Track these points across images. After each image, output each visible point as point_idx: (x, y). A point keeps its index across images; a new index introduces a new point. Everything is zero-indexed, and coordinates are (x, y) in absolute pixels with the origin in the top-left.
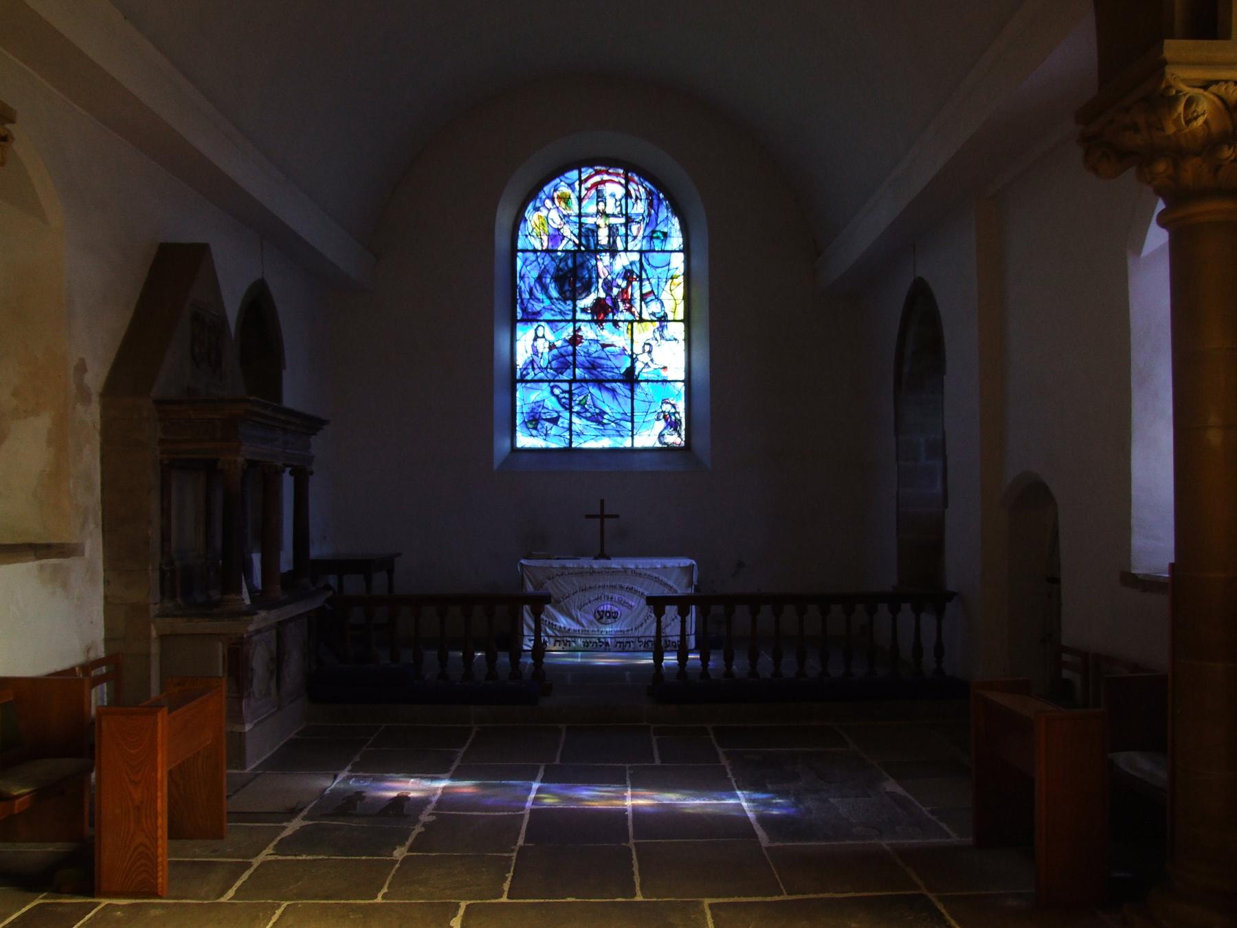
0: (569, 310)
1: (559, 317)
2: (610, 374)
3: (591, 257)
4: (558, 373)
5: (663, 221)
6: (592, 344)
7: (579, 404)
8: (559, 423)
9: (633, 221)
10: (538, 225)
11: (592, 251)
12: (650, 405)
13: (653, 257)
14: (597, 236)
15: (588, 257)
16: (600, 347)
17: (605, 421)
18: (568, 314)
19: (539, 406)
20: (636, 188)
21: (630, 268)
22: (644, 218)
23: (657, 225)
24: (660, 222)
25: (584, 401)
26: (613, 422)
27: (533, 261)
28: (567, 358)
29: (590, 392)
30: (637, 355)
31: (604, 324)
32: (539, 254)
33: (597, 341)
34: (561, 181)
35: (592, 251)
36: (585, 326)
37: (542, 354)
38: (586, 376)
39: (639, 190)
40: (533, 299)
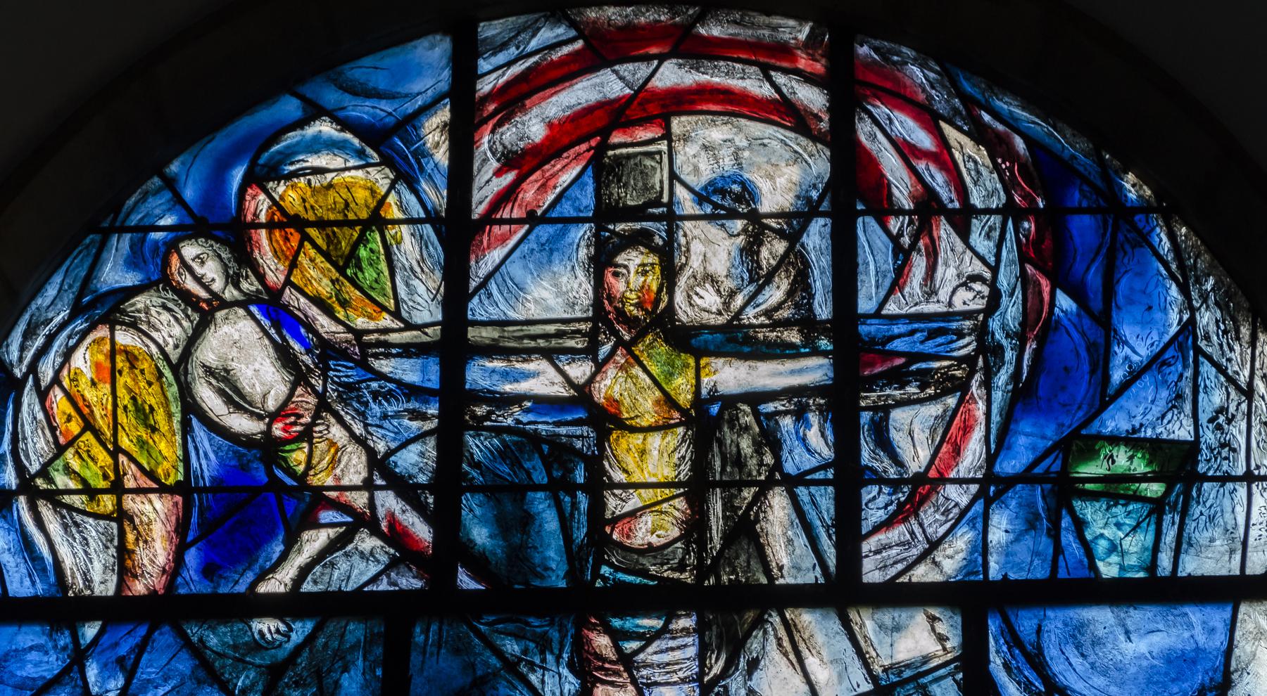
3: (544, 645)
5: (1157, 362)
9: (898, 377)
10: (103, 424)
13: (1076, 635)
14: (598, 485)
15: (512, 647)
20: (924, 140)
22: (989, 350)
23: (1105, 398)
24: (1135, 375)
32: (90, 631)
34: (315, 111)
39: (943, 157)
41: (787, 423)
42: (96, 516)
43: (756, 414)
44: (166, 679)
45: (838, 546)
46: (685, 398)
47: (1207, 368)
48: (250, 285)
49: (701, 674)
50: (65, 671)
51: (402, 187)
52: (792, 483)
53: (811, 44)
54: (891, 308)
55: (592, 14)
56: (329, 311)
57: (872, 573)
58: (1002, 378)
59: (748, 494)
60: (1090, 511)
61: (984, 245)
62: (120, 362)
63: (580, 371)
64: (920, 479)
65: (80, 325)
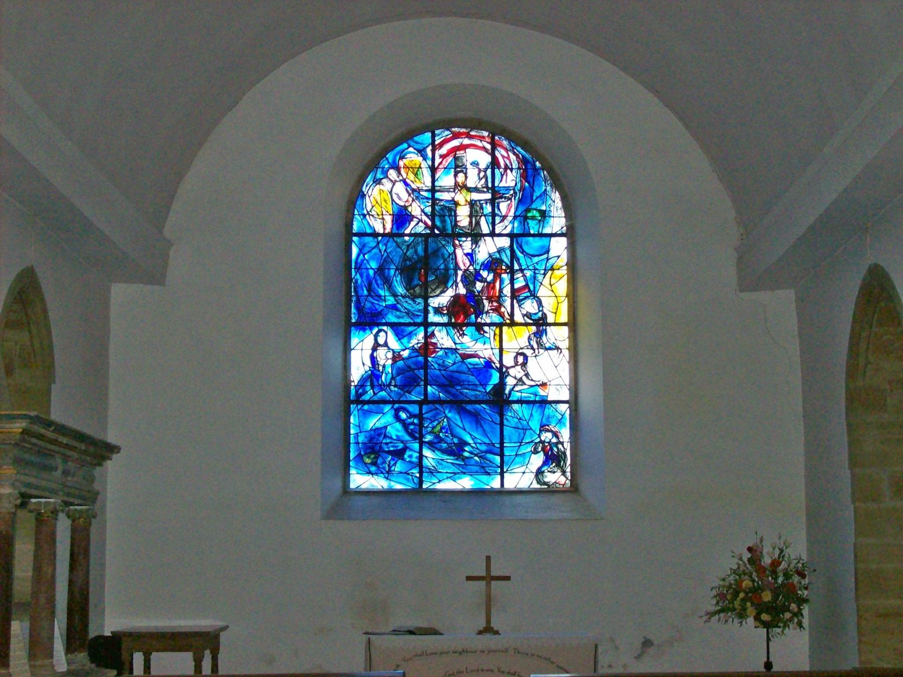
0: (419, 311)
1: (408, 320)
2: (473, 393)
4: (405, 392)
5: (540, 196)
6: (450, 354)
7: (430, 433)
8: (406, 456)
9: (501, 198)
10: (379, 202)
11: (448, 235)
12: (525, 434)
13: (527, 243)
14: (456, 216)
15: (444, 243)
16: (459, 358)
17: (466, 454)
18: (418, 316)
19: (379, 435)
20: (506, 155)
21: (498, 256)
22: (515, 193)
23: (532, 202)
25: (438, 428)
26: (476, 455)
27: (374, 248)
28: (416, 371)
29: (446, 417)
30: (507, 368)
31: (464, 329)
32: (380, 238)
33: (456, 349)
34: (409, 146)
35: (448, 235)
36: (440, 331)
37: (384, 366)
38: (441, 395)
39: (508, 158)
40: (372, 296)
41: (484, 205)
42: (380, 219)
43: (480, 203)
44: (392, 247)
45: (492, 226)
46: (469, 200)
47: (548, 197)
48: (401, 178)
49: (471, 248)
50: (376, 246)
51: (424, 161)
52: (485, 216)
53: (488, 136)
54: (500, 186)
55: (453, 129)
56: (413, 183)
57: (497, 231)
58: (517, 198)
59: (478, 217)
60: (530, 221)
61: (515, 174)
62: (381, 191)
63: (453, 194)
64: (504, 216)
65: (374, 185)
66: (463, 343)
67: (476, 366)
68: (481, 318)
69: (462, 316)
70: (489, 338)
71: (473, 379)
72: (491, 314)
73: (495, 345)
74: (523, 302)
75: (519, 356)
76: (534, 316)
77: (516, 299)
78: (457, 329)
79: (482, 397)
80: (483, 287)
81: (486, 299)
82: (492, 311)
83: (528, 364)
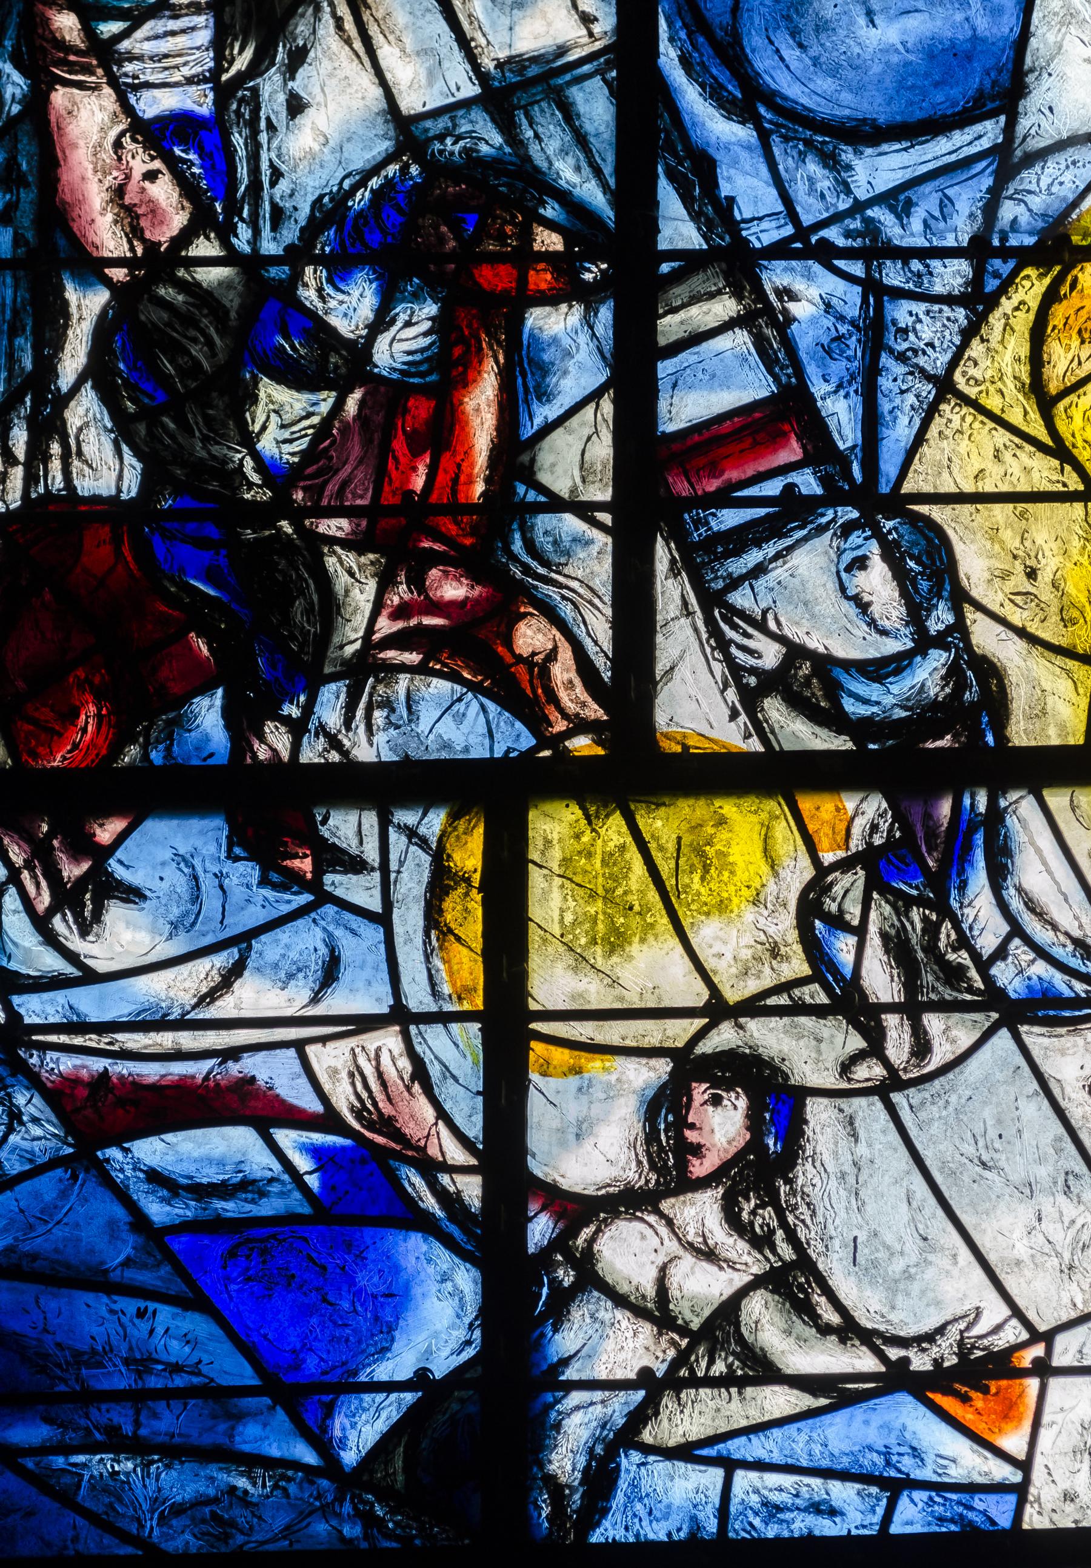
31: (105, 834)
66: (90, 977)
67: (230, 1208)
68: (297, 729)
69: (88, 716)
70: (383, 919)
71: (187, 1339)
72: (403, 682)
73: (446, 989)
74: (753, 557)
75: (700, 1092)
76: (873, 690)
77: (678, 535)
78: (27, 837)
79: (280, 1521)
80: (323, 430)
81: (354, 544)
82: (413, 658)
83: (805, 1173)
